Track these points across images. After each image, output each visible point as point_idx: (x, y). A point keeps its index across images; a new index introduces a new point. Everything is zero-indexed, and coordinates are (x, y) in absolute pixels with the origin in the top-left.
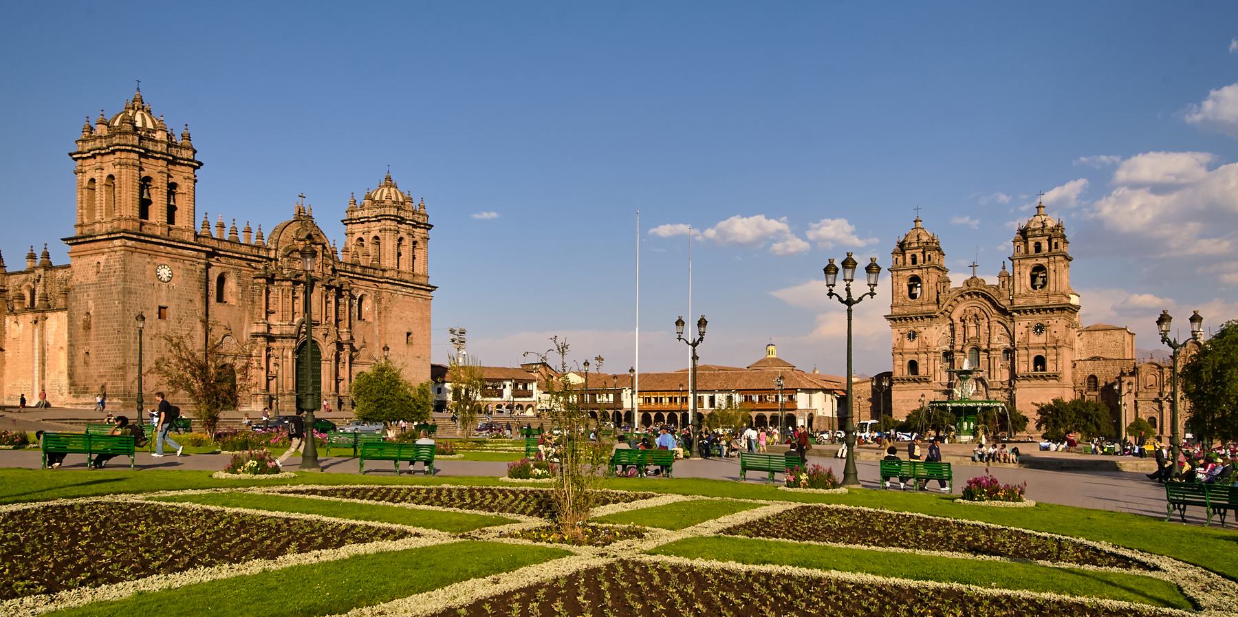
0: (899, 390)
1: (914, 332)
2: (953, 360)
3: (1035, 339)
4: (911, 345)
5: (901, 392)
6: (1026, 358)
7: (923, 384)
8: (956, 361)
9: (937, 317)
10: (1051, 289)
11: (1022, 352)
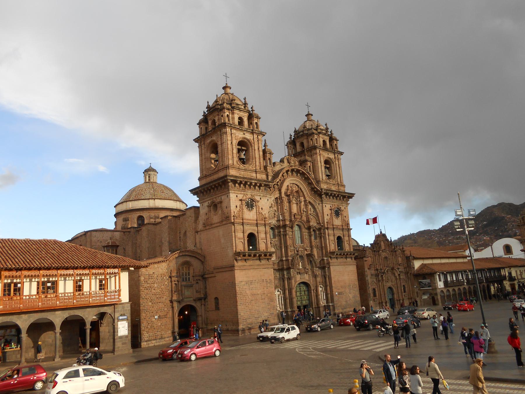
0: (242, 269)
1: (253, 200)
2: (285, 235)
3: (337, 222)
4: (250, 215)
5: (244, 272)
6: (332, 238)
7: (263, 262)
8: (288, 237)
9: (270, 188)
10: (339, 181)
11: (331, 232)
